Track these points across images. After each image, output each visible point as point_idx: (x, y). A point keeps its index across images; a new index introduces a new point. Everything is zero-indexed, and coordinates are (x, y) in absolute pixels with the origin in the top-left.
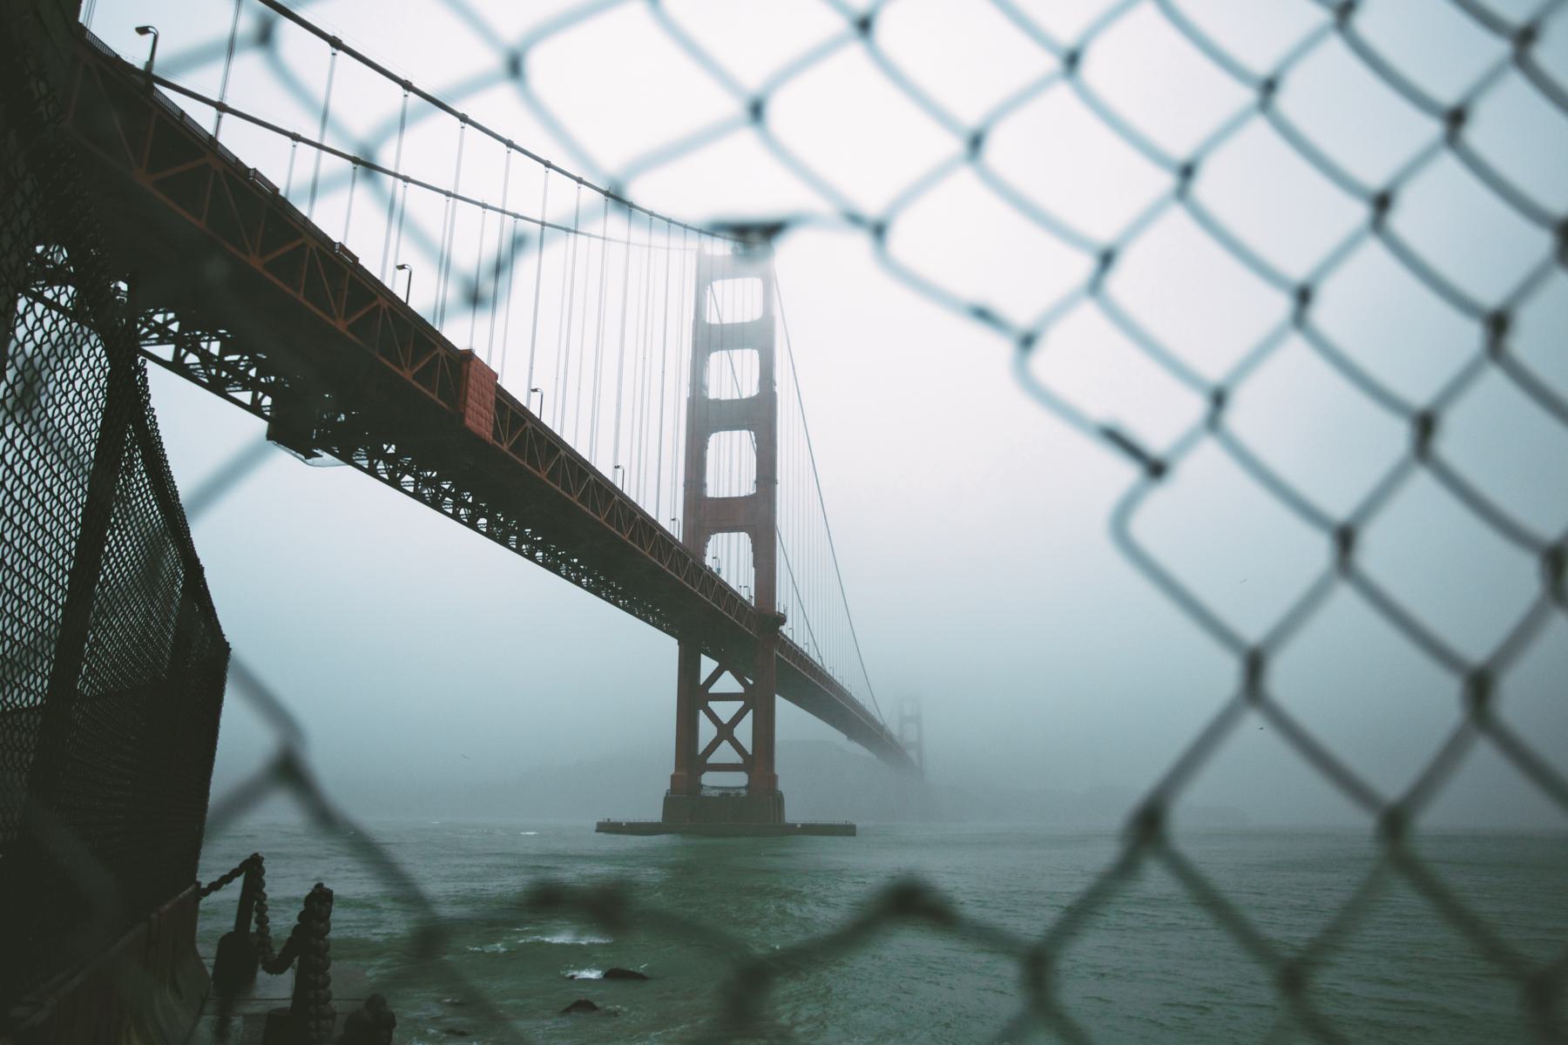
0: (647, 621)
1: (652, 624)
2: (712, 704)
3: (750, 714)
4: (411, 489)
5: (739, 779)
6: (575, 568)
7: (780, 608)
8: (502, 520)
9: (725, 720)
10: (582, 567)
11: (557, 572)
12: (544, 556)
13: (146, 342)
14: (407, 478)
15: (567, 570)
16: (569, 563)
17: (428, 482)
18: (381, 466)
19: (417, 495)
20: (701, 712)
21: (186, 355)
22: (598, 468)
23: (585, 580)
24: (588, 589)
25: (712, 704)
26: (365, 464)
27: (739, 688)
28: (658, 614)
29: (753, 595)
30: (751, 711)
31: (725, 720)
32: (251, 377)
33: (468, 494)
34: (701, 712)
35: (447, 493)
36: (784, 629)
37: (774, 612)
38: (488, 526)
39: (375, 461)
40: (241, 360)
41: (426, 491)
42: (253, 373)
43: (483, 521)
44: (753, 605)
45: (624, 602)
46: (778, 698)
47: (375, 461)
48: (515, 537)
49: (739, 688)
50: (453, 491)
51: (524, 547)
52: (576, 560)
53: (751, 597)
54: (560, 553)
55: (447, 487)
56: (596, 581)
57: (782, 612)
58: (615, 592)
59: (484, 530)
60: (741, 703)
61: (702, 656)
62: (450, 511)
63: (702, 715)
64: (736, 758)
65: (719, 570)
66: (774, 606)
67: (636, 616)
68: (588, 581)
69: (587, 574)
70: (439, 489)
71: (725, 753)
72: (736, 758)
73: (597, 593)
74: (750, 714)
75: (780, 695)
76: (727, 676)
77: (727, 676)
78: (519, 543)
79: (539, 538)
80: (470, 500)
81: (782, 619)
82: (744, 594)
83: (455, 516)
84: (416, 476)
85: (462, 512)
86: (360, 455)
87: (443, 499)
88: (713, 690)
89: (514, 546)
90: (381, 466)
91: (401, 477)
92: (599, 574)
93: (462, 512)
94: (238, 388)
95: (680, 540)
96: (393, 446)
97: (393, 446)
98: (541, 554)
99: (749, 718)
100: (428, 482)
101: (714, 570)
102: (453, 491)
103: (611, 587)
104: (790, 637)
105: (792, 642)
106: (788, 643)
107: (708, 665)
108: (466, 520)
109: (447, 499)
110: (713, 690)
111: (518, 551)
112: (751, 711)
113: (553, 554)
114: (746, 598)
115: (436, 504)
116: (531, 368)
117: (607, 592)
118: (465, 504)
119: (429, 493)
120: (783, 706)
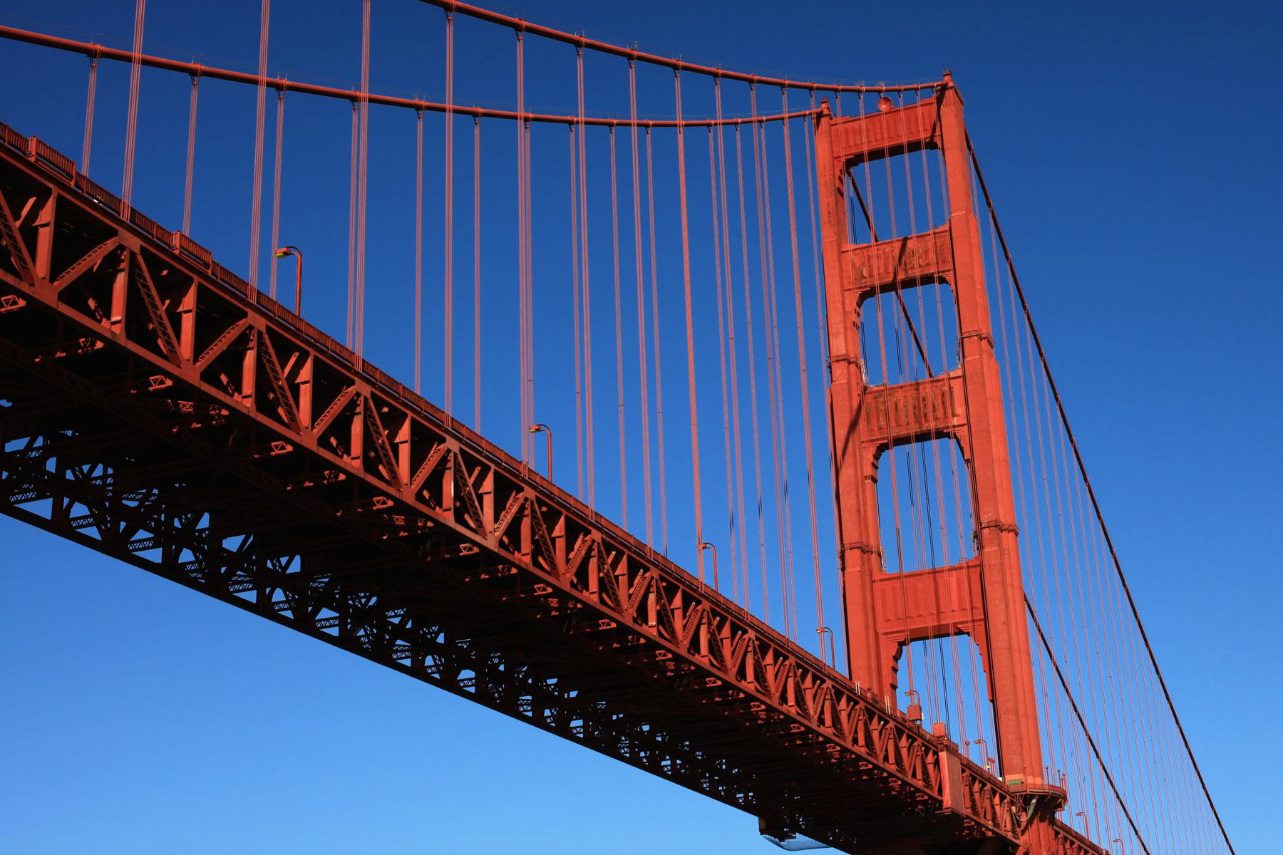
4: (335, 632)
6: (646, 742)
8: (502, 668)
11: (613, 752)
12: (585, 726)
13: (19, 497)
14: (325, 613)
15: (631, 747)
17: (363, 617)
18: (279, 595)
19: (346, 642)
21: (70, 505)
23: (668, 763)
24: (675, 777)
26: (251, 596)
32: (49, 473)
33: (435, 629)
35: (399, 631)
36: (1063, 816)
38: (478, 681)
39: (268, 590)
40: (29, 447)
41: (362, 632)
42: (51, 465)
43: (467, 674)
45: (746, 797)
47: (268, 590)
48: (530, 698)
50: (409, 625)
51: (547, 713)
52: (646, 728)
53: (993, 761)
54: (614, 717)
55: (396, 621)
56: (688, 758)
59: (472, 690)
62: (408, 662)
68: (673, 765)
69: (665, 749)
70: (383, 625)
78: (538, 706)
79: (573, 694)
80: (441, 639)
83: (418, 672)
84: (341, 607)
85: (429, 661)
86: (241, 583)
87: (392, 642)
89: (530, 714)
90: (279, 595)
91: (316, 611)
92: (694, 748)
93: (429, 661)
94: (30, 495)
96: (297, 559)
97: (297, 559)
98: (580, 723)
100: (363, 617)
102: (409, 625)
108: (437, 676)
109: (399, 642)
111: (538, 721)
115: (381, 654)
117: (711, 781)
118: (434, 649)
119: (366, 636)
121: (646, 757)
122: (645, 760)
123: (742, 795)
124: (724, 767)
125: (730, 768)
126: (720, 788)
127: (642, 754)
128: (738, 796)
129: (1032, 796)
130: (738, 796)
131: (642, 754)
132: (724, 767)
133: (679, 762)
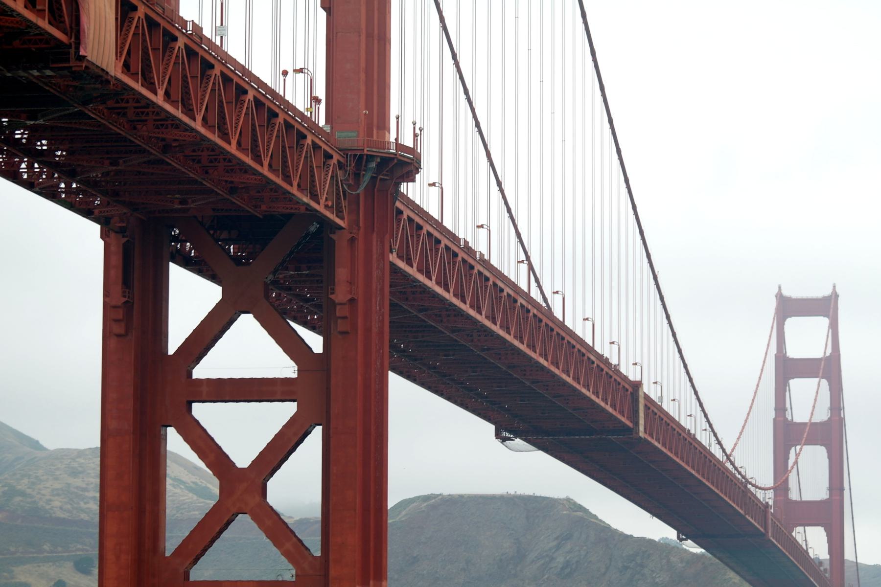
1: (29, 185)
3: (317, 434)
29: (321, 92)
30: (318, 431)
36: (412, 190)
37: (385, 144)
44: (322, 122)
46: (397, 385)
53: (317, 100)
66: (384, 125)
74: (317, 434)
75: (401, 373)
104: (435, 213)
105: (439, 225)
106: (427, 228)
114: (300, 102)
116: (800, 490)
129: (370, 158)
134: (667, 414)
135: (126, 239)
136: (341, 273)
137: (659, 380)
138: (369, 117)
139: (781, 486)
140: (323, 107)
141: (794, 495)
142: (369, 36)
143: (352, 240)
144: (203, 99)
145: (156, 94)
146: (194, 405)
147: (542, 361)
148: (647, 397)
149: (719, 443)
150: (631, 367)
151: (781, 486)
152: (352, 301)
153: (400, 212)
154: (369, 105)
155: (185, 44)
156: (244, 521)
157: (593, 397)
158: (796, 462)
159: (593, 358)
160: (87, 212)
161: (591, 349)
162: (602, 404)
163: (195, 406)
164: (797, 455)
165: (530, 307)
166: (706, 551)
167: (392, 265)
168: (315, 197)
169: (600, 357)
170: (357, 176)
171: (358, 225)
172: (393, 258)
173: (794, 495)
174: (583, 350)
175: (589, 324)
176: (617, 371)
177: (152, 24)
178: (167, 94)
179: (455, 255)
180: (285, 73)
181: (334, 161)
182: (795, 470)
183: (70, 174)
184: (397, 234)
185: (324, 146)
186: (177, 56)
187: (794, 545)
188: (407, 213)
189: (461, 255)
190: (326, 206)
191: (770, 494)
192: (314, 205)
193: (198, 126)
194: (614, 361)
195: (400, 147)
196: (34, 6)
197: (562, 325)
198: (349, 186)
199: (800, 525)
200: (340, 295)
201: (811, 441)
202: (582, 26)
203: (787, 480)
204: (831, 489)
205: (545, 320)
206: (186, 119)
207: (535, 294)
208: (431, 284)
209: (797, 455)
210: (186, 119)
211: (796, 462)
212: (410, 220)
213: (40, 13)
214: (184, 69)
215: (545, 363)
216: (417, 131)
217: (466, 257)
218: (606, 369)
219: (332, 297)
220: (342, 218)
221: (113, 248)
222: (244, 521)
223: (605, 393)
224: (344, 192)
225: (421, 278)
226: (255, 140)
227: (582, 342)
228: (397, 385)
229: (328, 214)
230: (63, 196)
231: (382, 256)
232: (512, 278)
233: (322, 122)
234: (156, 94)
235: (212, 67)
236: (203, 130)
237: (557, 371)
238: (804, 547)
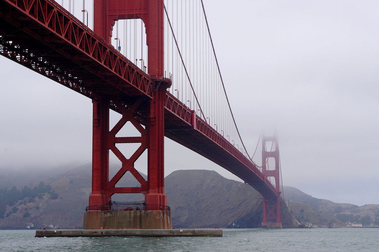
0: (67, 85)
1: (72, 88)
2: (118, 146)
3: (146, 151)
5: (140, 197)
7: (167, 76)
9: (128, 156)
10: (16, 47)
16: (37, 61)
20: (110, 151)
22: (64, 7)
24: (21, 63)
25: (118, 146)
27: (138, 134)
28: (76, 81)
29: (146, 64)
30: (147, 149)
31: (128, 156)
34: (110, 151)
44: (147, 73)
45: (49, 73)
49: (137, 134)
52: (11, 42)
53: (145, 67)
57: (169, 78)
58: (42, 64)
60: (140, 144)
61: (110, 109)
63: (111, 153)
64: (137, 184)
65: (120, 48)
67: (58, 82)
68: (21, 58)
69: (18, 51)
71: (128, 180)
72: (137, 184)
73: (28, 65)
74: (146, 151)
76: (129, 124)
77: (129, 124)
81: (168, 83)
82: (139, 65)
88: (118, 135)
92: (30, 52)
95: (91, 26)
99: (145, 154)
101: (115, 48)
103: (40, 62)
107: (114, 117)
110: (118, 135)
112: (147, 149)
113: (54, 71)
117: (36, 65)
120: (170, 145)
121: (10, 54)
122: (9, 55)
123: (48, 72)
124: (41, 60)
125: (44, 61)
126: (39, 68)
127: (9, 52)
128: (46, 72)
130: (46, 72)
131: (9, 52)
132: (41, 60)
133: (23, 57)
134: (235, 148)
135: (98, 103)
136: (152, 110)
137: (228, 135)
138: (159, 72)
139: (264, 167)
140: (147, 69)
141: (267, 169)
142: (159, 52)
143: (155, 103)
144: (132, 78)
145: (101, 62)
146: (116, 144)
147: (204, 134)
148: (197, 116)
149: (249, 156)
150: (227, 137)
151: (264, 167)
152: (155, 117)
153: (167, 96)
154: (158, 69)
155: (110, 51)
156: (128, 173)
157: (217, 144)
158: (268, 160)
159: (217, 134)
160: (88, 95)
161: (216, 132)
162: (219, 145)
163: (116, 144)
164: (268, 159)
165: (201, 121)
166: (246, 181)
167: (165, 109)
168: (145, 91)
169: (219, 134)
170: (156, 86)
171: (156, 98)
172: (165, 107)
173: (267, 169)
174: (214, 132)
175: (216, 126)
176: (223, 137)
177: (100, 45)
178: (115, 70)
179: (182, 107)
180: (137, 60)
181: (150, 83)
182: (267, 163)
183: (82, 86)
184: (167, 101)
185: (147, 78)
186: (107, 54)
187: (267, 181)
188: (169, 96)
189: (183, 107)
190: (148, 94)
191: (261, 168)
192: (144, 93)
193: (113, 71)
194: (222, 135)
195: (166, 78)
196: (68, 38)
197: (209, 126)
198: (154, 89)
199: (268, 176)
200: (152, 116)
201: (271, 156)
202: (214, 53)
203: (265, 165)
204: (276, 168)
205: (205, 124)
206: (110, 70)
207: (202, 118)
208: (175, 114)
209: (268, 159)
210: (110, 70)
211: (268, 160)
212: (170, 98)
213: (69, 40)
214: (109, 57)
215: (205, 135)
216: (171, 75)
217: (184, 108)
218: (220, 137)
219: (150, 116)
220: (152, 97)
221: (95, 105)
222: (128, 173)
223: (220, 143)
224: (152, 90)
225: (173, 112)
226: (129, 76)
227: (214, 130)
228: (165, 137)
229: (148, 95)
230: (81, 91)
231: (162, 106)
232: (181, 101)
233: (147, 73)
234: (101, 62)
235: (134, 70)
236: (114, 72)
237: (208, 137)
238: (270, 181)
